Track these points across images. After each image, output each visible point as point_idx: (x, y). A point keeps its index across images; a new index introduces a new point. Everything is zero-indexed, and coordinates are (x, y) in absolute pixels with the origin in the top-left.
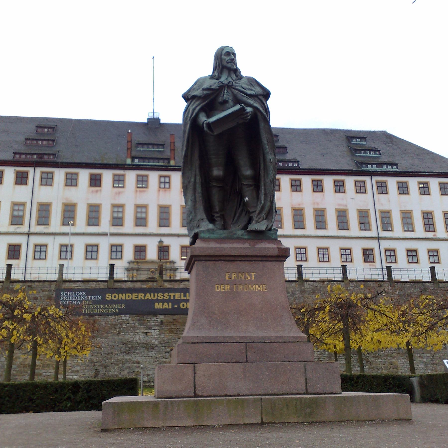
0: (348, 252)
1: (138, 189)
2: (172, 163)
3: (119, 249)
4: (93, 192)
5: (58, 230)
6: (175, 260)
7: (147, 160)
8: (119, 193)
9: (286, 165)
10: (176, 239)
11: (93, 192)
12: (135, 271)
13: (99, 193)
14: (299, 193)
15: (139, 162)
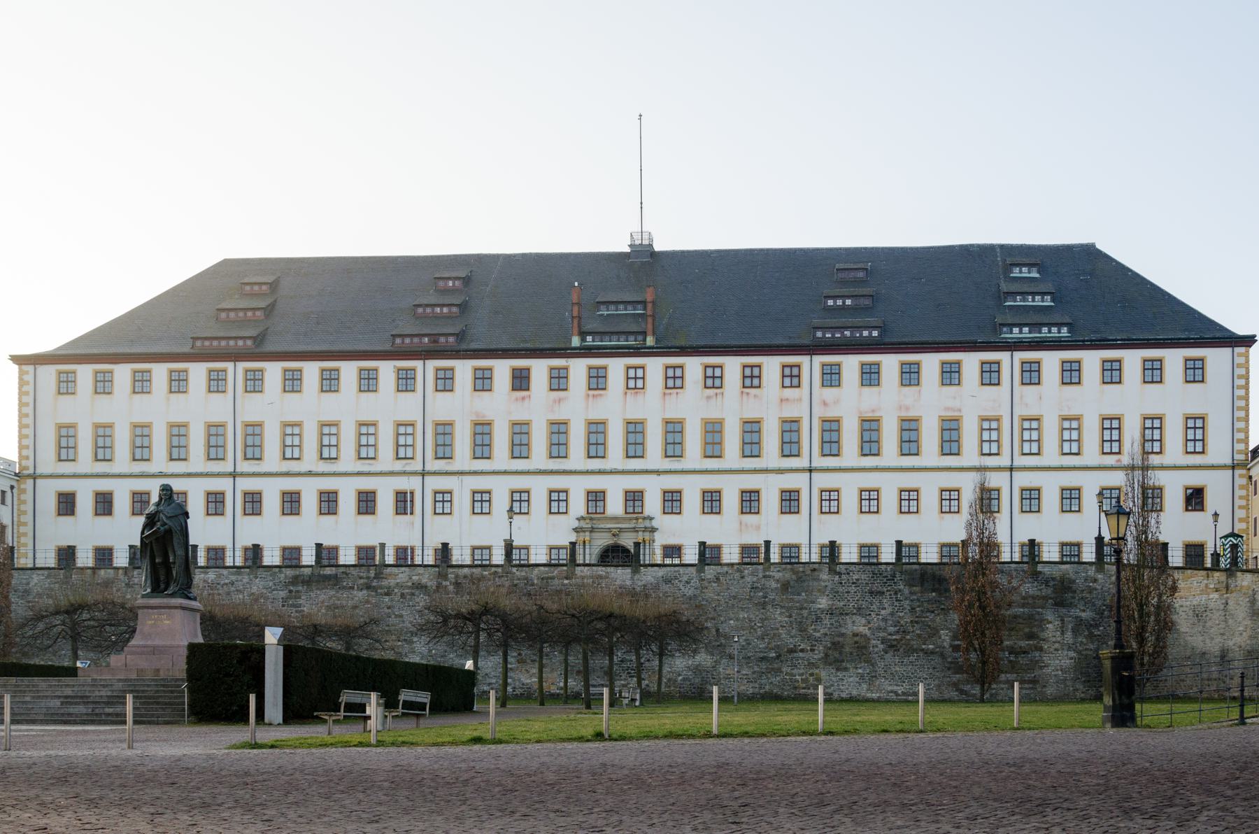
0: (954, 495)
1: (592, 392)
2: (650, 341)
3: (563, 496)
4: (517, 399)
5: (467, 468)
6: (652, 515)
7: (607, 338)
8: (560, 400)
9: (858, 335)
10: (654, 476)
11: (517, 399)
12: (587, 534)
13: (527, 401)
14: (875, 389)
15: (593, 341)
